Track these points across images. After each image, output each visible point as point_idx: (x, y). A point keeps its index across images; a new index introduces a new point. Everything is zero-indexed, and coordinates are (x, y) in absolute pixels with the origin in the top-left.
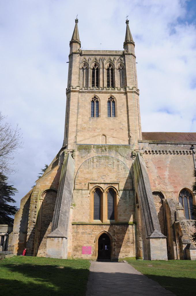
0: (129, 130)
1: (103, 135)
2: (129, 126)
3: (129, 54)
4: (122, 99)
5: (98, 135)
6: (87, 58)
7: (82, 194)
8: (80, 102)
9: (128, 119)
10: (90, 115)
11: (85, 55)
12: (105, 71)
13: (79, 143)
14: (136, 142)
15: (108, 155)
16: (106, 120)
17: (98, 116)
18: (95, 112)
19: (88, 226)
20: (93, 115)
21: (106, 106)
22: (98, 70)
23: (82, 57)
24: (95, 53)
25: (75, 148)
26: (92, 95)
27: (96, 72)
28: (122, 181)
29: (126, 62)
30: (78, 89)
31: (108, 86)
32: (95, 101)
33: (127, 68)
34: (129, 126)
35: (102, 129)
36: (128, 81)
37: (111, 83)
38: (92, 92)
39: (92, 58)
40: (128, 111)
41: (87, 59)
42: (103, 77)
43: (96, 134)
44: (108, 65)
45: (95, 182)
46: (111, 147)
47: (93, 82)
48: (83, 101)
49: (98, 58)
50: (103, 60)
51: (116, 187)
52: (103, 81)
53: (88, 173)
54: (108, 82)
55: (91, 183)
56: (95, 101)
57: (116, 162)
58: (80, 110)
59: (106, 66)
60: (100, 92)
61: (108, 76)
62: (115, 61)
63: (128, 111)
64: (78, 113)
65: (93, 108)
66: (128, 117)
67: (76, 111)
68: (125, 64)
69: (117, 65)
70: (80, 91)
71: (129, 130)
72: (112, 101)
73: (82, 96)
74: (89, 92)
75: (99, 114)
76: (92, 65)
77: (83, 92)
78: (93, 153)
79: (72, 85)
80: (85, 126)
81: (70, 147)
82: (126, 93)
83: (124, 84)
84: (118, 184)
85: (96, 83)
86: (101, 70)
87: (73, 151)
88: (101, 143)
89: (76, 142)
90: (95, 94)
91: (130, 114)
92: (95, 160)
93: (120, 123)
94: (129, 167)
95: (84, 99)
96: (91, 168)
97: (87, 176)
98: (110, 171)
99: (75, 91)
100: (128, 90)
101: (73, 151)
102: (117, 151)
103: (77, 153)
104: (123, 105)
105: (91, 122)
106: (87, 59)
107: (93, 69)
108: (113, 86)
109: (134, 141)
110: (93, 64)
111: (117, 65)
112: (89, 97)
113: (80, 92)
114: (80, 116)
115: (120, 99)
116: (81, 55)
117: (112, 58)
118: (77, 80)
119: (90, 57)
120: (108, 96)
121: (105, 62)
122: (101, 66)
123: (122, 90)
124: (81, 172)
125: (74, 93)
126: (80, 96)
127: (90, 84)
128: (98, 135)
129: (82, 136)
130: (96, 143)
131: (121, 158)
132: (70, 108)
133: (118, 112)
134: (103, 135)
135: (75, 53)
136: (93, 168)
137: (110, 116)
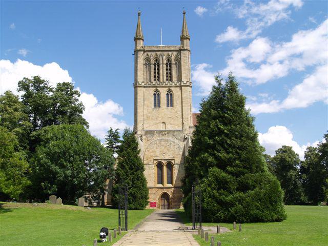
0: (182, 118)
1: (163, 123)
2: (182, 115)
3: (184, 50)
4: (177, 92)
5: (159, 123)
6: (149, 54)
7: (149, 167)
9: (182, 109)
10: (153, 106)
11: (147, 51)
12: (165, 66)
13: (146, 129)
14: (188, 128)
15: (167, 138)
16: (165, 110)
17: (159, 106)
18: (157, 104)
19: (154, 189)
20: (155, 106)
21: (166, 98)
23: (146, 53)
25: (143, 133)
28: (177, 158)
30: (143, 84)
31: (167, 80)
32: (157, 95)
33: (182, 63)
34: (182, 115)
35: (163, 118)
36: (183, 75)
37: (170, 78)
38: (154, 87)
39: (154, 54)
40: (182, 102)
43: (158, 122)
45: (158, 158)
46: (169, 132)
47: (155, 76)
49: (159, 53)
50: (162, 56)
51: (173, 162)
52: (163, 76)
53: (153, 152)
54: (167, 75)
55: (155, 160)
57: (173, 143)
58: (145, 102)
59: (165, 62)
60: (160, 87)
61: (167, 70)
62: (173, 57)
63: (182, 102)
64: (144, 105)
65: (155, 99)
66: (182, 107)
67: (142, 103)
68: (181, 59)
71: (182, 118)
74: (151, 87)
76: (153, 62)
77: (147, 87)
78: (156, 136)
79: (138, 81)
80: (150, 115)
81: (139, 133)
82: (181, 87)
83: (179, 78)
84: (174, 159)
87: (142, 136)
88: (162, 129)
89: (143, 129)
91: (183, 105)
92: (158, 142)
93: (176, 112)
94: (182, 147)
95: (148, 93)
96: (155, 148)
97: (152, 154)
98: (169, 150)
99: (141, 87)
100: (182, 84)
101: (142, 136)
102: (173, 135)
103: (144, 137)
104: (179, 97)
105: (154, 112)
108: (171, 80)
109: (186, 127)
113: (144, 87)
114: (145, 107)
115: (176, 91)
116: (144, 51)
117: (170, 53)
118: (142, 75)
119: (152, 53)
121: (164, 57)
122: (161, 62)
124: (148, 151)
128: (159, 123)
129: (147, 124)
130: (158, 129)
131: (177, 141)
133: (175, 102)
134: (163, 123)
135: (140, 50)
136: (157, 148)
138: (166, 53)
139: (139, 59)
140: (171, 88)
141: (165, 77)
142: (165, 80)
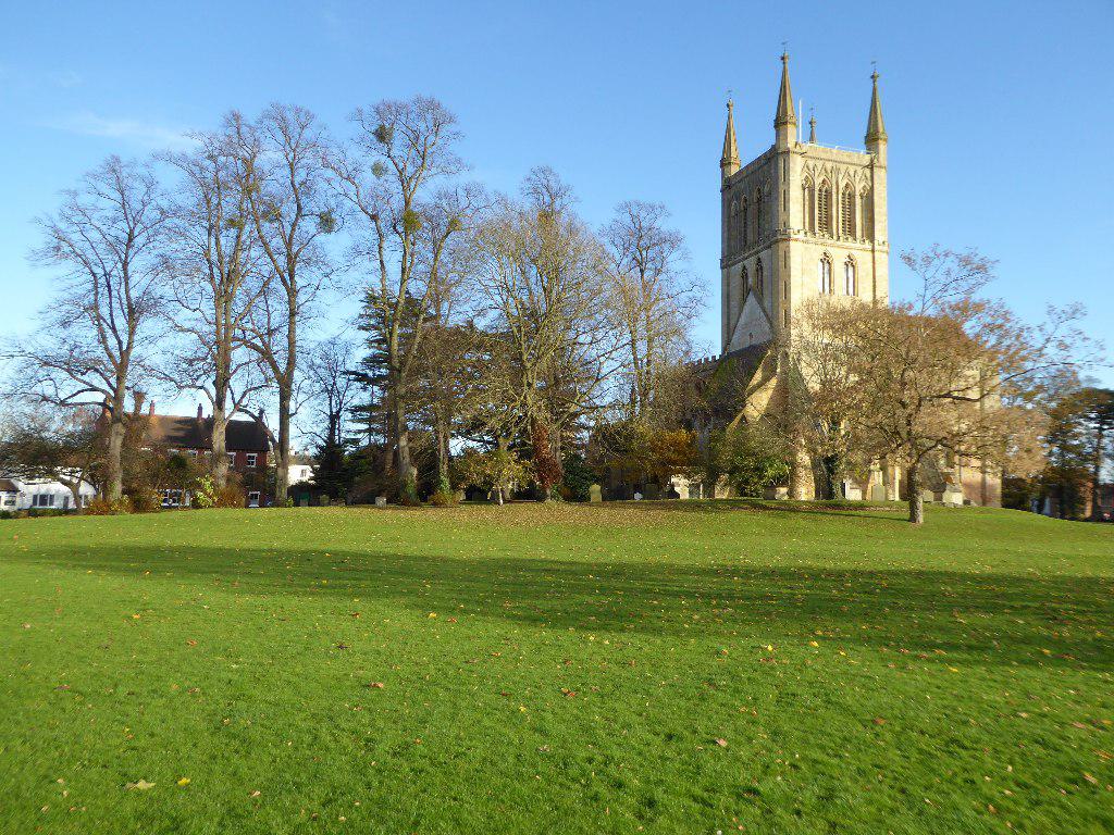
6: (811, 163)
12: (840, 195)
22: (828, 194)
24: (823, 156)
26: (822, 249)
32: (826, 260)
33: (876, 198)
36: (878, 227)
39: (819, 164)
41: (811, 167)
42: (837, 213)
56: (826, 260)
60: (832, 246)
68: (872, 188)
69: (859, 188)
72: (850, 263)
73: (806, 248)
76: (818, 181)
79: (792, 225)
85: (826, 224)
100: (877, 247)
104: (867, 275)
106: (811, 167)
107: (820, 190)
111: (859, 188)
112: (818, 252)
120: (847, 252)
121: (840, 177)
123: (868, 245)
138: (845, 166)
140: (853, 252)
142: (841, 231)
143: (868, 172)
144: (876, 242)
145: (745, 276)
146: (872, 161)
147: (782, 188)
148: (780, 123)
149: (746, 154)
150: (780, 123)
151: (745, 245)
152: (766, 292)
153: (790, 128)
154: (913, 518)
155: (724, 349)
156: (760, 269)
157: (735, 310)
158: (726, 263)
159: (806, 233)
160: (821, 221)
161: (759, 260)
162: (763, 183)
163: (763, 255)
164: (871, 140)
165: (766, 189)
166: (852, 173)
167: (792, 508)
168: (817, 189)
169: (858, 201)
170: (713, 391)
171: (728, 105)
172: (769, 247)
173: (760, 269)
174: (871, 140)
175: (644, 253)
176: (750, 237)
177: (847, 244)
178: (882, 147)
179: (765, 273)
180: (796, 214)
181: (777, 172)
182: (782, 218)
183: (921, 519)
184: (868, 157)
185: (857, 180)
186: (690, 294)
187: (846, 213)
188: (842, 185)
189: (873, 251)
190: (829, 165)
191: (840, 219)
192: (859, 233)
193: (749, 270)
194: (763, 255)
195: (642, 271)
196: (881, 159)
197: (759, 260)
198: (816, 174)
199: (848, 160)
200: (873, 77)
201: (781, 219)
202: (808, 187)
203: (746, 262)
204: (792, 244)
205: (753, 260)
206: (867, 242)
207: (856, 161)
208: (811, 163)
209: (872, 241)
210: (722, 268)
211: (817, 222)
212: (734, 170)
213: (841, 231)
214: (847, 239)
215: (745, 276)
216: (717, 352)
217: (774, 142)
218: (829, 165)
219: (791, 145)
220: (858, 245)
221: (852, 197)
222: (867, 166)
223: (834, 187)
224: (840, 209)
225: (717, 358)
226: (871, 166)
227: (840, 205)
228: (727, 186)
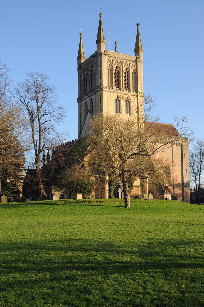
8: (109, 100)
12: (124, 73)
24: (117, 56)
26: (116, 95)
27: (118, 73)
29: (138, 69)
33: (138, 74)
36: (139, 86)
37: (128, 87)
42: (122, 80)
44: (126, 67)
48: (110, 99)
56: (118, 100)
67: (107, 107)
69: (132, 70)
70: (109, 90)
72: (128, 101)
75: (120, 111)
79: (103, 84)
85: (118, 85)
86: (121, 73)
90: (118, 94)
100: (139, 94)
106: (111, 61)
107: (115, 70)
110: (116, 66)
111: (132, 70)
115: (133, 99)
120: (125, 97)
121: (124, 65)
123: (135, 93)
125: (105, 92)
126: (108, 94)
127: (114, 86)
132: (103, 104)
137: (127, 113)
139: (103, 63)
140: (130, 96)
141: (124, 85)
142: (124, 88)
143: (135, 63)
144: (138, 92)
145: (86, 106)
146: (137, 59)
147: (99, 69)
148: (99, 41)
149: (87, 54)
150: (99, 41)
151: (86, 94)
152: (94, 112)
153: (102, 44)
154: (126, 206)
155: (79, 136)
156: (92, 103)
157: (83, 120)
158: (80, 100)
159: (109, 88)
160: (116, 83)
161: (91, 99)
162: (92, 67)
163: (93, 97)
164: (137, 50)
165: (94, 69)
166: (128, 64)
167: (55, 203)
168: (114, 70)
169: (131, 75)
170: (67, 156)
171: (80, 34)
172: (95, 94)
173: (92, 103)
174: (137, 50)
175: (38, 95)
176: (88, 89)
177: (126, 93)
178: (141, 53)
179: (93, 104)
180: (105, 80)
181: (97, 61)
182: (100, 81)
183: (129, 206)
184: (135, 57)
185: (131, 66)
186: (57, 112)
187: (125, 79)
188: (125, 68)
189: (137, 96)
190: (119, 60)
191: (124, 83)
192: (131, 89)
193: (88, 103)
194: (93, 97)
195: (37, 103)
196: (140, 58)
197: (91, 99)
198: (114, 64)
199: (126, 58)
200: (137, 24)
201: (99, 83)
202: (110, 69)
203: (87, 100)
204: (103, 91)
205: (89, 98)
206: (135, 92)
207: (130, 59)
208: (111, 59)
209: (137, 92)
210: (78, 102)
211: (114, 84)
212: (83, 61)
213: (124, 88)
214: (127, 91)
215: (86, 106)
216: (77, 138)
217: (96, 50)
218: (119, 60)
219: (103, 51)
220: (130, 93)
221: (128, 73)
222: (135, 61)
223: (121, 69)
224: (124, 78)
225: (77, 140)
226: (136, 61)
227: (124, 77)
228: (80, 68)
